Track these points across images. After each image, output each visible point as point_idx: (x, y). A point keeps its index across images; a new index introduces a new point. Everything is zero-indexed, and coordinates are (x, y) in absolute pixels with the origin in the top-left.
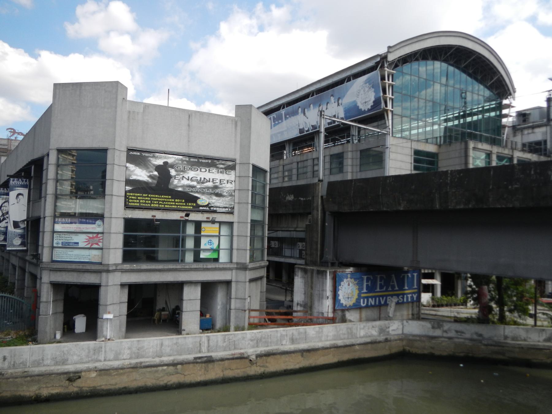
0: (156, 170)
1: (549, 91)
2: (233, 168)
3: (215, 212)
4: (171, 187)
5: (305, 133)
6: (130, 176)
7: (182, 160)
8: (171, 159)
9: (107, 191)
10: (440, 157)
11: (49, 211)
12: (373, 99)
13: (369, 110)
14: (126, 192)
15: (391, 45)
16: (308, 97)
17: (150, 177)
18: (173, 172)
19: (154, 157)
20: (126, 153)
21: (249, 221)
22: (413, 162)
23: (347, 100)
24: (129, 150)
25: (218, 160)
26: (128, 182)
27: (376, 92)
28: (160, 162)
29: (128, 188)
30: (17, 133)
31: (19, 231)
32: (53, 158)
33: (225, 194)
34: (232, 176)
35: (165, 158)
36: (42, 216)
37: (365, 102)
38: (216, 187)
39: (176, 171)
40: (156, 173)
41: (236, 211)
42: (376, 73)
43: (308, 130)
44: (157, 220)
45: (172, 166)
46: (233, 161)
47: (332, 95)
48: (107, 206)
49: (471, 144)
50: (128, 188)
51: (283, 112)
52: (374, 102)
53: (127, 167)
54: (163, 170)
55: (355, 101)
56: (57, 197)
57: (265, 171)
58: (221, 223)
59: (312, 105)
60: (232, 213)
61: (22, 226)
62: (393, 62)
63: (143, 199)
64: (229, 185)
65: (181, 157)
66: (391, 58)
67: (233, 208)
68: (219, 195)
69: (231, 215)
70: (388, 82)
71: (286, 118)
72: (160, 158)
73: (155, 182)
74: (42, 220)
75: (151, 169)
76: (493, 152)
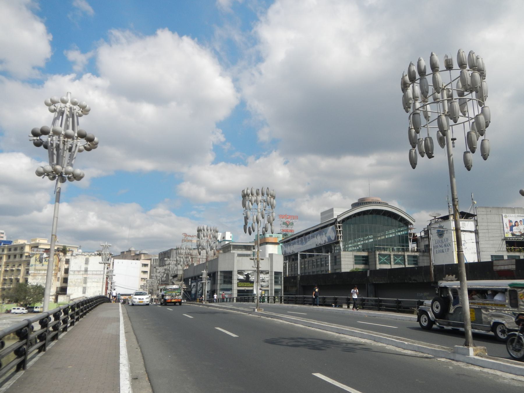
0: (245, 276)
1: (431, 220)
2: (268, 273)
3: (263, 287)
4: (250, 280)
5: (318, 246)
6: (238, 278)
7: (252, 272)
8: (249, 272)
9: (233, 283)
10: (370, 257)
11: (218, 288)
12: (334, 236)
13: (334, 240)
14: (238, 282)
15: (338, 215)
16: (318, 230)
17: (244, 278)
18: (250, 276)
19: (245, 272)
20: (237, 272)
21: (273, 289)
22: (354, 261)
23: (328, 235)
24: (238, 271)
25: (263, 271)
26: (238, 280)
27: (335, 234)
28: (246, 273)
29: (238, 281)
30: (187, 235)
31: (209, 294)
32: (219, 273)
33: (266, 281)
34: (268, 275)
35: (248, 272)
36: (216, 289)
37: (333, 237)
38: (263, 279)
39: (251, 275)
40: (245, 277)
41: (269, 286)
42: (334, 226)
43: (318, 245)
44: (246, 290)
45: (250, 274)
46: (268, 271)
47: (324, 232)
48: (233, 287)
49: (377, 253)
50: (238, 281)
51: (310, 235)
52: (335, 237)
53: (238, 276)
54: (247, 276)
55: (330, 236)
56: (220, 284)
57: (281, 273)
58: (265, 290)
59: (318, 235)
60: (268, 287)
61: (209, 292)
62: (340, 221)
63: (242, 284)
64: (267, 278)
65: (252, 271)
66: (339, 220)
67: (269, 285)
68: (264, 282)
69: (268, 288)
70: (340, 229)
71: (312, 238)
72: (246, 272)
73: (245, 279)
74: (216, 291)
75: (244, 275)
76: (391, 254)
